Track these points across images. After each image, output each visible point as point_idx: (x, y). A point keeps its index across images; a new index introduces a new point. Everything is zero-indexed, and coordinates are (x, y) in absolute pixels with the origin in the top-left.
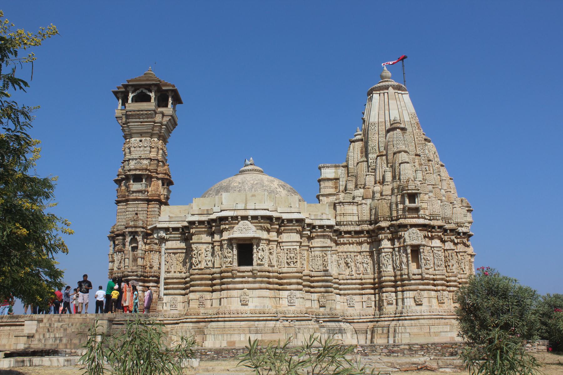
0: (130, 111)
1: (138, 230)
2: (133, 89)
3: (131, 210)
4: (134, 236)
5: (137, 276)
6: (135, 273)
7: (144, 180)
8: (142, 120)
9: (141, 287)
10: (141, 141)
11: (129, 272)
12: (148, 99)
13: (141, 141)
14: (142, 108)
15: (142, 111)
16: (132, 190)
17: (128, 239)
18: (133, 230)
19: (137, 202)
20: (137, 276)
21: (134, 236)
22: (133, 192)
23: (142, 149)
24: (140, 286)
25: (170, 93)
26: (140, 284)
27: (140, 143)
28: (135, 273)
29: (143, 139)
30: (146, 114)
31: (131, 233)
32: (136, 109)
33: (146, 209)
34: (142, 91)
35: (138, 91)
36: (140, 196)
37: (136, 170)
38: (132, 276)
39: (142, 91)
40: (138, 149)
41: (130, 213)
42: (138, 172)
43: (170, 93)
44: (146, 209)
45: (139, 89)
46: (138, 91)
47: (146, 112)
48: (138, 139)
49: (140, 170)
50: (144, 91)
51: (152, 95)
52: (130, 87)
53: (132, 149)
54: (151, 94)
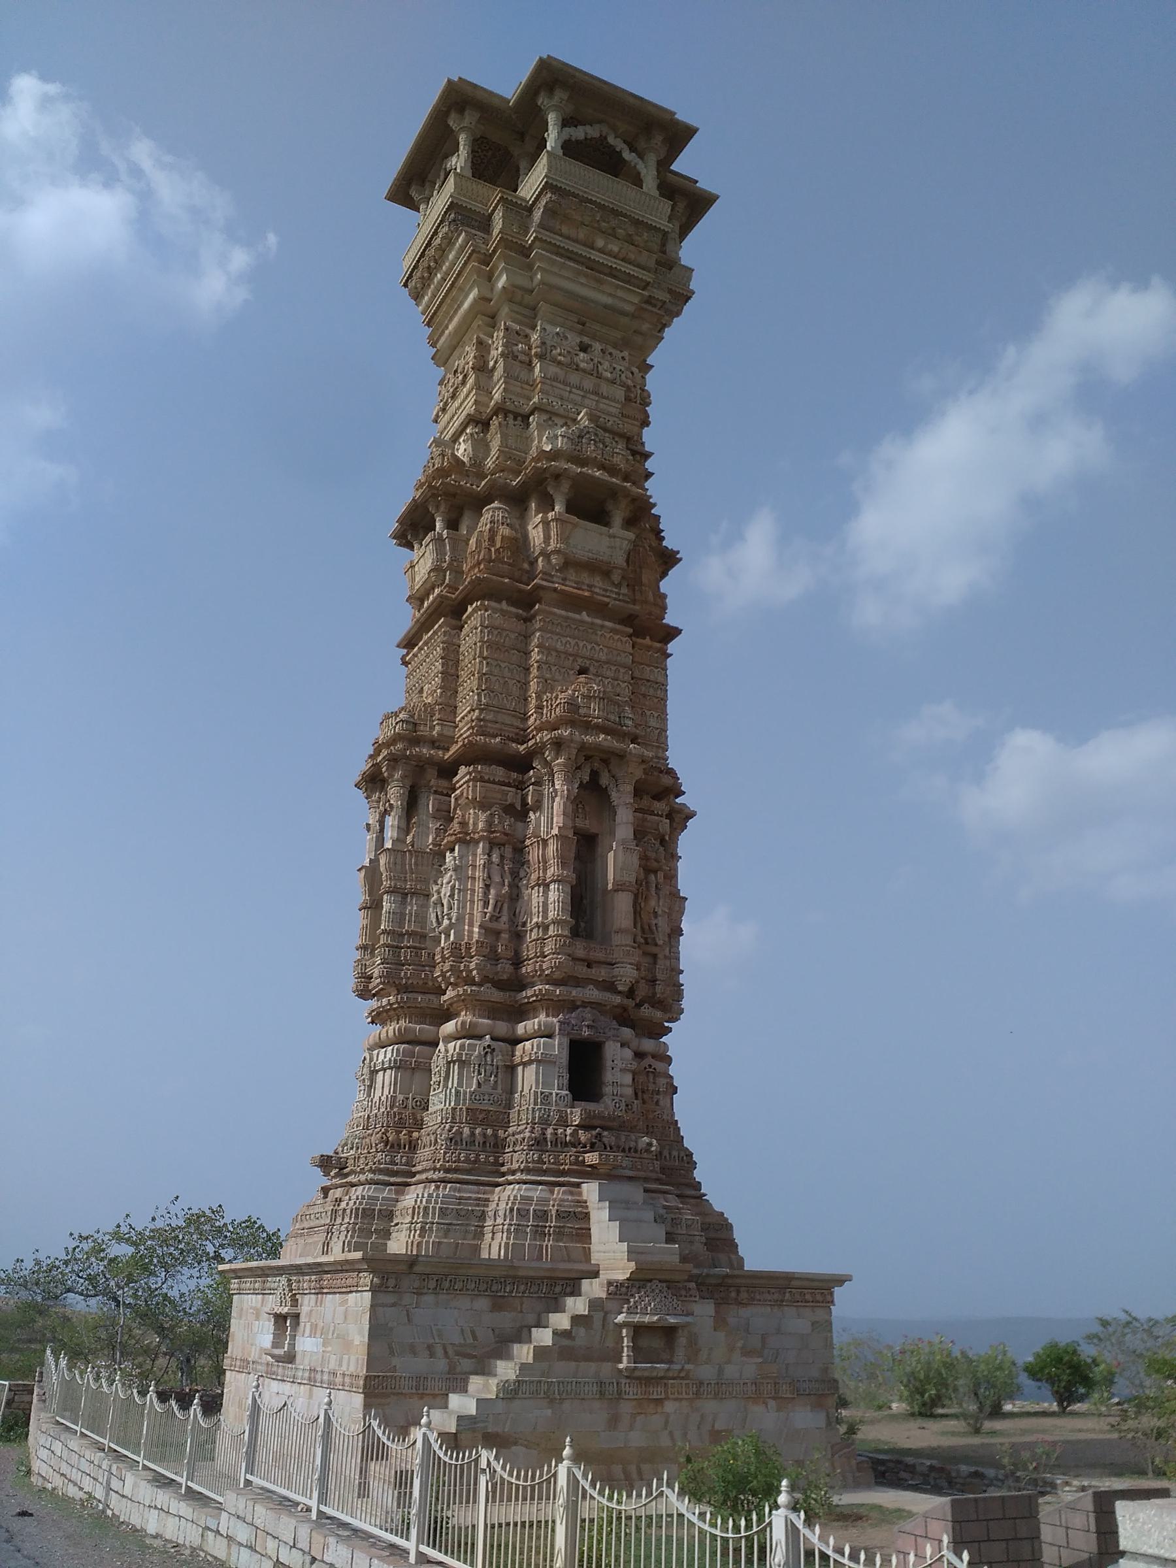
4: (594, 775)
5: (609, 986)
7: (617, 519)
8: (595, 256)
10: (584, 348)
15: (616, 213)
20: (609, 986)
21: (594, 775)
23: (588, 383)
26: (627, 1032)
29: (597, 346)
34: (603, 139)
39: (603, 139)
40: (574, 378)
46: (593, 132)
48: (574, 339)
49: (602, 467)
50: (611, 140)
52: (560, 95)
54: (641, 166)
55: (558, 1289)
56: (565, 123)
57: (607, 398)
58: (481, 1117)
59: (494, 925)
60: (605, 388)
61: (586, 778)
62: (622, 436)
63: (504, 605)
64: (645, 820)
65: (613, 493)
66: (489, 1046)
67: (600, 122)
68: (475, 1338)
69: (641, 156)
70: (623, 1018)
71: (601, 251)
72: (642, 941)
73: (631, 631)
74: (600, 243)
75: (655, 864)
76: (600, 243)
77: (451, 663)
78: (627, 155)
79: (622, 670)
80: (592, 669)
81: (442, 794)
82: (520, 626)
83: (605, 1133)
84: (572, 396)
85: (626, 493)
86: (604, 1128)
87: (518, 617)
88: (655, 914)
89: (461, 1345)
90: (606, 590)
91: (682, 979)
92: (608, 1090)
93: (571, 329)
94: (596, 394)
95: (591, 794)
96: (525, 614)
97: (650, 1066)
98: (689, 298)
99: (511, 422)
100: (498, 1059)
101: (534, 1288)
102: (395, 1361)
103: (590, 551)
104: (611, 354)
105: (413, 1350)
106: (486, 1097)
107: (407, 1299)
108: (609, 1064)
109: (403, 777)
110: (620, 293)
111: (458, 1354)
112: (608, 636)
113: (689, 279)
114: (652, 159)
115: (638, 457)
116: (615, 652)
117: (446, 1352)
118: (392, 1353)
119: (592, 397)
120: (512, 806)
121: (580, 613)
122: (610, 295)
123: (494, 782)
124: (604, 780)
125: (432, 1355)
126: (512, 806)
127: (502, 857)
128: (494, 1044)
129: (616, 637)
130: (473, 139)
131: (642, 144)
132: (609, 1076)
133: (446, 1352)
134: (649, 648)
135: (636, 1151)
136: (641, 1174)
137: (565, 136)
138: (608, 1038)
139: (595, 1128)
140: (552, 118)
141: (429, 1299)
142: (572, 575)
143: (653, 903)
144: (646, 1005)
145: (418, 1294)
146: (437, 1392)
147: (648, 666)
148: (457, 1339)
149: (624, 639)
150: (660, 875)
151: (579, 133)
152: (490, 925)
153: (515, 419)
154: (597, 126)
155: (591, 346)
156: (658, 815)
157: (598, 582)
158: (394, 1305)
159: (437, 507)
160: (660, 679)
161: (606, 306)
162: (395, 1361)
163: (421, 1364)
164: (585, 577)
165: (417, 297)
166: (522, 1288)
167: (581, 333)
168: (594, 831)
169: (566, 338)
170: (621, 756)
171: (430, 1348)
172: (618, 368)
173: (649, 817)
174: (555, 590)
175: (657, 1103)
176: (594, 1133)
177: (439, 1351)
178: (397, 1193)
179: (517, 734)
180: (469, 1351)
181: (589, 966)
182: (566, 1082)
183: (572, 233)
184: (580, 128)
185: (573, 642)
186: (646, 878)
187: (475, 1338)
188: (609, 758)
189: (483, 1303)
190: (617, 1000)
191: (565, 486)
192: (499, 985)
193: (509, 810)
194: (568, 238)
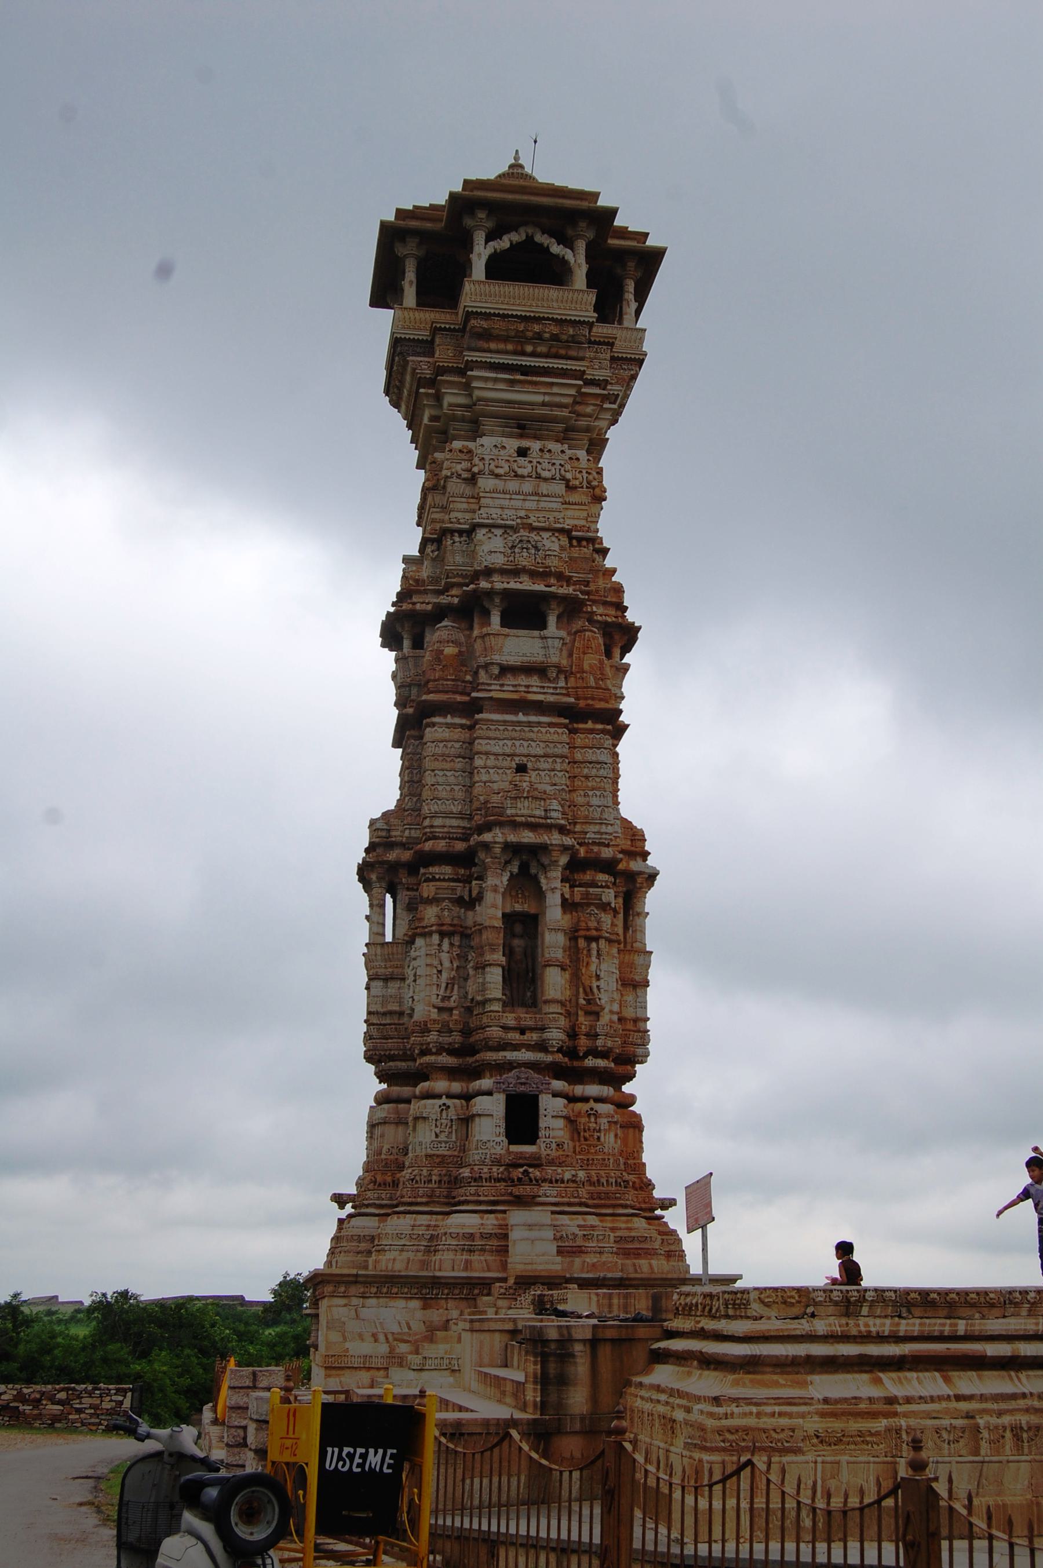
0: (487, 316)
1: (544, 838)
2: (490, 225)
3: (497, 749)
4: (524, 868)
5: (542, 1047)
6: (535, 1036)
7: (552, 620)
9: (561, 1102)
10: (522, 452)
11: (505, 1028)
12: (555, 274)
13: (522, 452)
14: (542, 311)
15: (537, 320)
16: (497, 658)
17: (497, 880)
18: (528, 837)
19: (521, 717)
22: (506, 670)
23: (528, 487)
24: (555, 1095)
25: (631, 265)
26: (558, 1085)
27: (521, 460)
28: (535, 1036)
29: (535, 445)
30: (555, 338)
31: (514, 849)
32: (519, 310)
33: (565, 750)
34: (530, 239)
35: (515, 237)
36: (536, 689)
37: (515, 572)
38: (516, 1047)
39: (530, 239)
40: (513, 485)
41: (491, 762)
42: (526, 584)
43: (631, 265)
44: (565, 750)
45: (515, 229)
46: (515, 237)
47: (555, 330)
48: (513, 444)
49: (533, 574)
50: (541, 238)
51: (578, 260)
53: (485, 483)
54: (569, 255)
55: (476, 1291)
56: (488, 239)
57: (548, 496)
58: (437, 1161)
59: (446, 1004)
60: (544, 488)
61: (516, 870)
62: (562, 531)
63: (449, 719)
64: (588, 893)
65: (544, 598)
66: (444, 1104)
67: (525, 224)
68: (409, 1328)
69: (569, 244)
70: (558, 1071)
71: (533, 354)
72: (584, 1002)
73: (567, 721)
74: (529, 349)
75: (594, 933)
76: (529, 349)
77: (415, 772)
78: (556, 249)
79: (558, 760)
80: (530, 765)
81: (412, 890)
82: (465, 735)
83: (531, 1170)
84: (513, 502)
85: (554, 596)
86: (530, 1166)
87: (462, 726)
88: (598, 978)
89: (399, 1334)
90: (543, 687)
91: (649, 1025)
92: (542, 1133)
93: (510, 436)
94: (537, 494)
95: (526, 881)
96: (468, 723)
97: (592, 1109)
98: (643, 360)
99: (457, 539)
100: (452, 1114)
101: (457, 1291)
102: (347, 1345)
103: (524, 655)
104: (549, 451)
105: (361, 1337)
106: (443, 1145)
107: (355, 1301)
108: (542, 1112)
109: (379, 879)
110: (555, 390)
111: (395, 1339)
112: (544, 730)
113: (642, 340)
114: (581, 246)
115: (584, 543)
116: (552, 745)
117: (387, 1339)
118: (345, 1339)
119: (532, 498)
120: (461, 898)
121: (516, 714)
122: (545, 394)
123: (444, 880)
124: (533, 871)
125: (376, 1341)
126: (461, 898)
127: (451, 945)
128: (449, 1102)
129: (552, 730)
130: (422, 257)
131: (570, 232)
132: (543, 1123)
133: (387, 1339)
134: (591, 731)
135: (563, 1182)
136: (566, 1200)
137: (489, 250)
138: (541, 1092)
139: (521, 1166)
140: (479, 237)
141: (373, 1301)
142: (510, 680)
143: (593, 968)
144: (590, 1058)
145: (363, 1297)
146: (379, 1366)
147: (591, 748)
148: (396, 1329)
149: (560, 731)
150: (602, 942)
151: (504, 243)
152: (441, 1005)
153: (460, 536)
154: (522, 230)
155: (529, 449)
156: (602, 887)
157: (534, 681)
158: (345, 1305)
159: (403, 627)
160: (604, 756)
161: (544, 404)
162: (347, 1345)
163: (366, 1348)
164: (523, 680)
165: (395, 404)
166: (446, 1291)
167: (521, 436)
168: (533, 911)
169: (504, 447)
170: (544, 848)
171: (375, 1336)
172: (558, 462)
173: (591, 890)
174: (491, 698)
175: (599, 1138)
176: (521, 1170)
177: (382, 1338)
178: (380, 1222)
179: (463, 834)
180: (405, 1338)
181: (523, 1033)
182: (502, 1130)
183: (501, 346)
184: (505, 238)
185: (509, 743)
186: (589, 946)
187: (409, 1328)
188: (537, 851)
189: (415, 1304)
190: (549, 1058)
191: (497, 600)
192: (451, 1052)
193: (460, 901)
194: (498, 352)
